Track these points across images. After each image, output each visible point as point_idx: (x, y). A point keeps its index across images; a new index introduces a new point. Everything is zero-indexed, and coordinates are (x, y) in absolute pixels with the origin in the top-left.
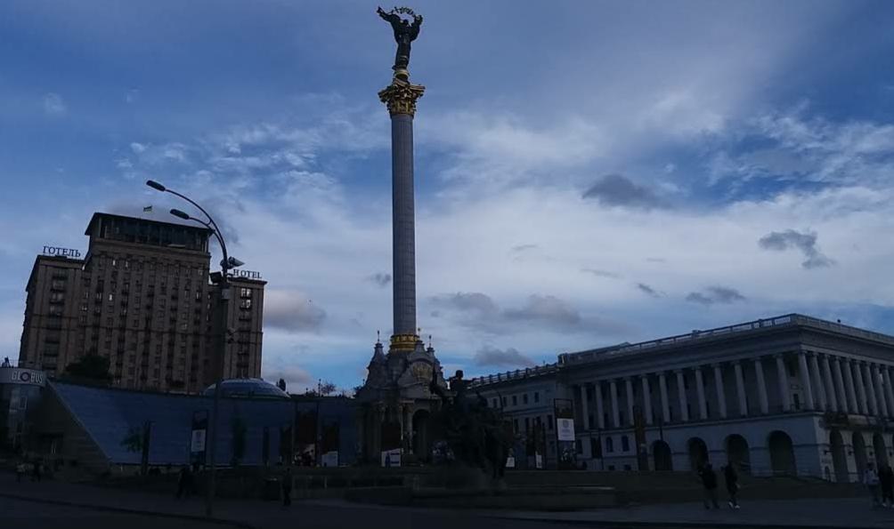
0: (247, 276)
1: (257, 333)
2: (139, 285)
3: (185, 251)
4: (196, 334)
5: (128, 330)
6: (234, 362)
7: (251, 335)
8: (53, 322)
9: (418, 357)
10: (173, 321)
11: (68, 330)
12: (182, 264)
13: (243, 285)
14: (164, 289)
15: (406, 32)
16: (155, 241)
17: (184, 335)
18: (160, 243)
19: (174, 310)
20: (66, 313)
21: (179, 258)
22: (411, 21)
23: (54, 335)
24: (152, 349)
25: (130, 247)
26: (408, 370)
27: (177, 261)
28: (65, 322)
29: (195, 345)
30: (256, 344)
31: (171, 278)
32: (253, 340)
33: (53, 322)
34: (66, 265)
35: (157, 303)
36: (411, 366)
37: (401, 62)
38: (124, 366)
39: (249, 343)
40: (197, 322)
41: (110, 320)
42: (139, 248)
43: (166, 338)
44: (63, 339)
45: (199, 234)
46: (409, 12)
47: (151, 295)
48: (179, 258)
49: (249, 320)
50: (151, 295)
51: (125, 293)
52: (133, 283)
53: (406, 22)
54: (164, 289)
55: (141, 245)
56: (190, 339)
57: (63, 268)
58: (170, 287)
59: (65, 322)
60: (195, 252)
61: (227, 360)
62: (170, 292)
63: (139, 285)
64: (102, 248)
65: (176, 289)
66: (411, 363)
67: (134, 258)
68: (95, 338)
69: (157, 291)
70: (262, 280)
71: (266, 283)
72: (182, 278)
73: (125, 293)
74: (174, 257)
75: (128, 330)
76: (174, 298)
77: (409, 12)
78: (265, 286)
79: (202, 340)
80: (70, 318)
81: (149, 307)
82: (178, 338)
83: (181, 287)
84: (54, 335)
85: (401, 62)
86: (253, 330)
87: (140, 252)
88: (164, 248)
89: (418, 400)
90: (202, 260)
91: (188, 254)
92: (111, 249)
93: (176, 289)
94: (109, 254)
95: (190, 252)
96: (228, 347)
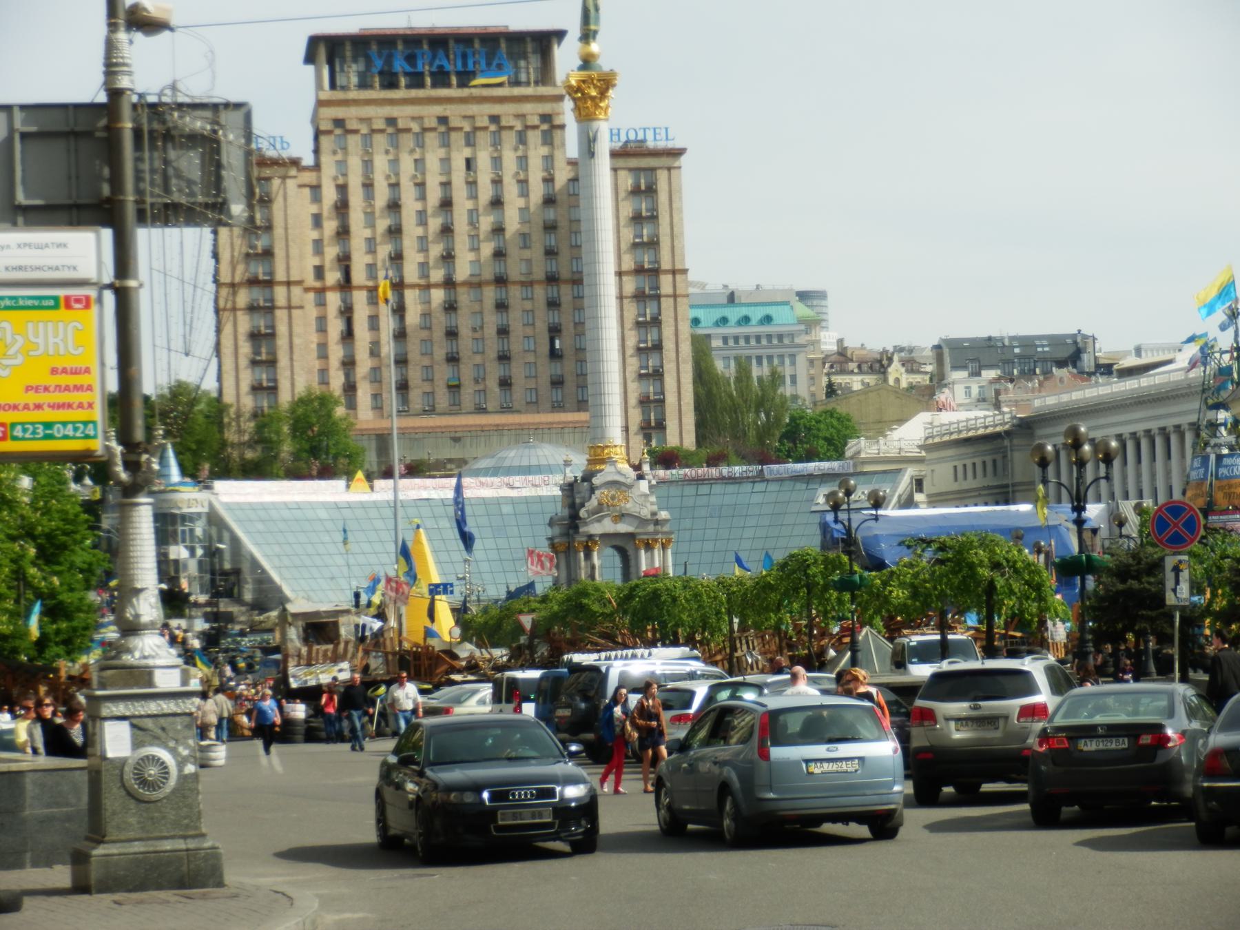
0: (641, 137)
1: (674, 272)
4: (552, 279)
5: (413, 286)
9: (610, 478)
11: (289, 308)
12: (504, 123)
13: (634, 163)
14: (472, 184)
16: (441, 79)
17: (528, 284)
18: (454, 80)
21: (496, 109)
24: (464, 323)
25: (392, 102)
26: (593, 497)
29: (553, 304)
30: (675, 296)
36: (597, 492)
38: (410, 366)
39: (658, 297)
40: (550, 253)
43: (490, 294)
44: (282, 329)
49: (653, 244)
51: (394, 206)
55: (414, 93)
56: (540, 293)
60: (529, 91)
63: (421, 185)
66: (597, 488)
67: (401, 125)
70: (677, 144)
74: (482, 112)
75: (413, 286)
76: (497, 203)
78: (684, 160)
80: (288, 284)
82: (515, 293)
86: (666, 264)
87: (410, 110)
88: (465, 92)
90: (546, 108)
93: (497, 182)
94: (351, 125)
95: (517, 91)
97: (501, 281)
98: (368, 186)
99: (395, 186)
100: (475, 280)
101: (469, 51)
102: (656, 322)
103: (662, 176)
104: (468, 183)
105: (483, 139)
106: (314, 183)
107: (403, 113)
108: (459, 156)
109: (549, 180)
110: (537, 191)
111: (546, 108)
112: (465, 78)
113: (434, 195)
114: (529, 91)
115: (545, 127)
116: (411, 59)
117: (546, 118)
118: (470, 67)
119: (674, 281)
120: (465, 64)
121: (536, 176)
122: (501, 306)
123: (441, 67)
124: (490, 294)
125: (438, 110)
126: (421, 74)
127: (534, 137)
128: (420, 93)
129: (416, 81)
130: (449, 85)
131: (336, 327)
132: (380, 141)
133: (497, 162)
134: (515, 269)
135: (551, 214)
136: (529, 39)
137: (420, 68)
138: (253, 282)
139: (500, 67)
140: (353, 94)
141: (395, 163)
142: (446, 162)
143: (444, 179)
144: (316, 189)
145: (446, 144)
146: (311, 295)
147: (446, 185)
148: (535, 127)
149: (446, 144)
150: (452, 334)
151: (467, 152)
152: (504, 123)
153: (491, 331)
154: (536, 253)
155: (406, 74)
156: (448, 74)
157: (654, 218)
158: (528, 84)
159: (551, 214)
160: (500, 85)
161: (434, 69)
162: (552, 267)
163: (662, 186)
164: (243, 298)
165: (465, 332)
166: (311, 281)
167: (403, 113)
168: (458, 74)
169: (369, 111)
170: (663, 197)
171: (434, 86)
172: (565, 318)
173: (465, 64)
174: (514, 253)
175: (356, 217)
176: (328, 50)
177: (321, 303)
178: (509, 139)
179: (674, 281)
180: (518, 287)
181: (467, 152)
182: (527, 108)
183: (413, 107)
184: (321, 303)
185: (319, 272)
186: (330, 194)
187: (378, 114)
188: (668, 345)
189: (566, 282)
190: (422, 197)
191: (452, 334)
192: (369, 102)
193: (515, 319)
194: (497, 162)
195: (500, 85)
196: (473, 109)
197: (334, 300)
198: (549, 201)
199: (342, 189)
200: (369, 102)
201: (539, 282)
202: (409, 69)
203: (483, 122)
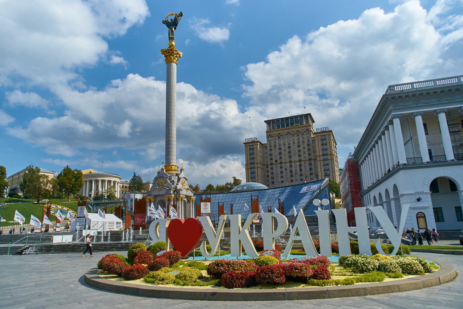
3: (300, 126)
4: (310, 160)
6: (323, 169)
8: (252, 166)
10: (300, 156)
13: (321, 134)
14: (294, 143)
15: (172, 24)
19: (299, 151)
20: (256, 162)
21: (298, 129)
22: (173, 17)
23: (253, 170)
24: (293, 169)
27: (298, 131)
28: (256, 165)
32: (329, 158)
33: (326, 157)
34: (253, 144)
35: (292, 150)
37: (171, 39)
40: (309, 154)
42: (281, 130)
43: (298, 163)
44: (256, 172)
46: (172, 15)
47: (289, 147)
48: (298, 129)
50: (289, 147)
51: (280, 149)
52: (282, 144)
53: (171, 20)
56: (307, 162)
58: (296, 142)
59: (256, 165)
61: (319, 170)
62: (296, 144)
63: (284, 144)
64: (270, 134)
68: (272, 168)
69: (291, 146)
70: (330, 130)
71: (331, 131)
72: (301, 138)
73: (280, 149)
76: (299, 146)
77: (172, 15)
81: (290, 152)
83: (301, 141)
84: (253, 170)
85: (171, 39)
86: (329, 154)
87: (282, 131)
89: (156, 196)
91: (301, 127)
92: (272, 133)
93: (298, 143)
97: (300, 161)
103: (327, 136)
107: (281, 132)
111: (307, 128)
112: (292, 124)
113: (287, 146)
117: (307, 130)
121: (306, 141)
122: (300, 166)
124: (298, 163)
125: (287, 131)
138: (251, 164)
144: (266, 147)
150: (291, 171)
152: (300, 131)
153: (298, 170)
154: (306, 155)
162: (310, 157)
163: (327, 138)
165: (294, 171)
170: (328, 140)
172: (313, 167)
174: (302, 155)
176: (268, 122)
178: (300, 134)
182: (304, 128)
187: (276, 133)
188: (331, 169)
191: (291, 171)
193: (303, 168)
196: (294, 130)
198: (308, 145)
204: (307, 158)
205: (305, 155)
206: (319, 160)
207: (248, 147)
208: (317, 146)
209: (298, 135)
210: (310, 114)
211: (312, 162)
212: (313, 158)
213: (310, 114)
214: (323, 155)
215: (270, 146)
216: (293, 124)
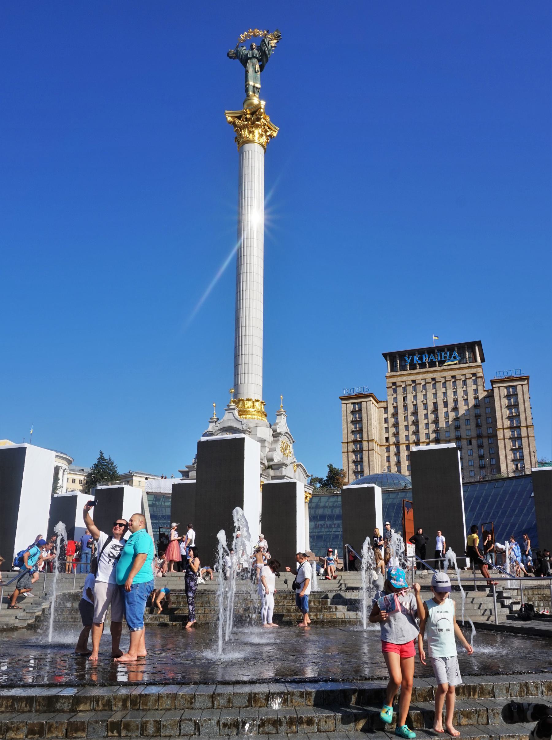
2: (425, 405)
4: (479, 437)
7: (522, 429)
16: (432, 364)
27: (453, 377)
29: (480, 446)
31: (450, 393)
41: (407, 437)
45: (468, 348)
51: (415, 413)
54: (446, 404)
55: (422, 370)
57: (358, 403)
60: (467, 365)
63: (425, 405)
65: (456, 401)
79: (485, 441)
88: (442, 368)
93: (456, 401)
95: (462, 366)
96: (501, 444)
98: (405, 406)
99: (415, 406)
100: (448, 439)
101: (443, 353)
102: (520, 448)
104: (444, 402)
105: (449, 385)
106: (386, 406)
107: (418, 378)
108: (440, 392)
109: (476, 398)
110: (472, 402)
112: (441, 363)
113: (431, 407)
114: (467, 365)
115: (474, 378)
116: (421, 359)
118: (443, 359)
119: (527, 431)
120: (441, 358)
123: (432, 360)
125: (431, 375)
126: (425, 363)
127: (470, 382)
128: (424, 370)
129: (423, 366)
130: (436, 366)
131: (394, 459)
132: (410, 389)
133: (455, 393)
134: (464, 433)
135: (478, 411)
136: (466, 346)
137: (424, 361)
139: (455, 357)
140: (399, 373)
141: (415, 397)
142: (435, 395)
143: (435, 401)
144: (386, 409)
145: (434, 387)
146: (384, 448)
147: (435, 404)
148: (471, 378)
149: (434, 387)
151: (444, 390)
152: (457, 377)
155: (419, 364)
156: (435, 362)
157: (516, 406)
158: (467, 363)
159: (478, 411)
160: (456, 364)
161: (430, 361)
164: (352, 447)
166: (384, 442)
167: (418, 378)
168: (439, 362)
169: (404, 378)
171: (429, 367)
173: (441, 358)
174: (463, 427)
175: (401, 417)
177: (388, 450)
179: (527, 431)
180: (465, 440)
181: (444, 390)
183: (421, 376)
184: (388, 450)
185: (387, 439)
186: (391, 410)
189: (486, 437)
190: (426, 408)
192: (404, 375)
194: (455, 393)
195: (456, 364)
196: (444, 374)
197: (393, 449)
199: (396, 408)
200: (404, 375)
201: (474, 438)
202: (420, 362)
203: (449, 378)
204: (474, 434)
205: (469, 427)
206: (502, 437)
207: (351, 407)
208: (498, 409)
209: (454, 383)
210: (479, 343)
211: (485, 441)
212: (485, 434)
213: (479, 343)
214: (511, 428)
215: (396, 408)
216: (444, 362)
